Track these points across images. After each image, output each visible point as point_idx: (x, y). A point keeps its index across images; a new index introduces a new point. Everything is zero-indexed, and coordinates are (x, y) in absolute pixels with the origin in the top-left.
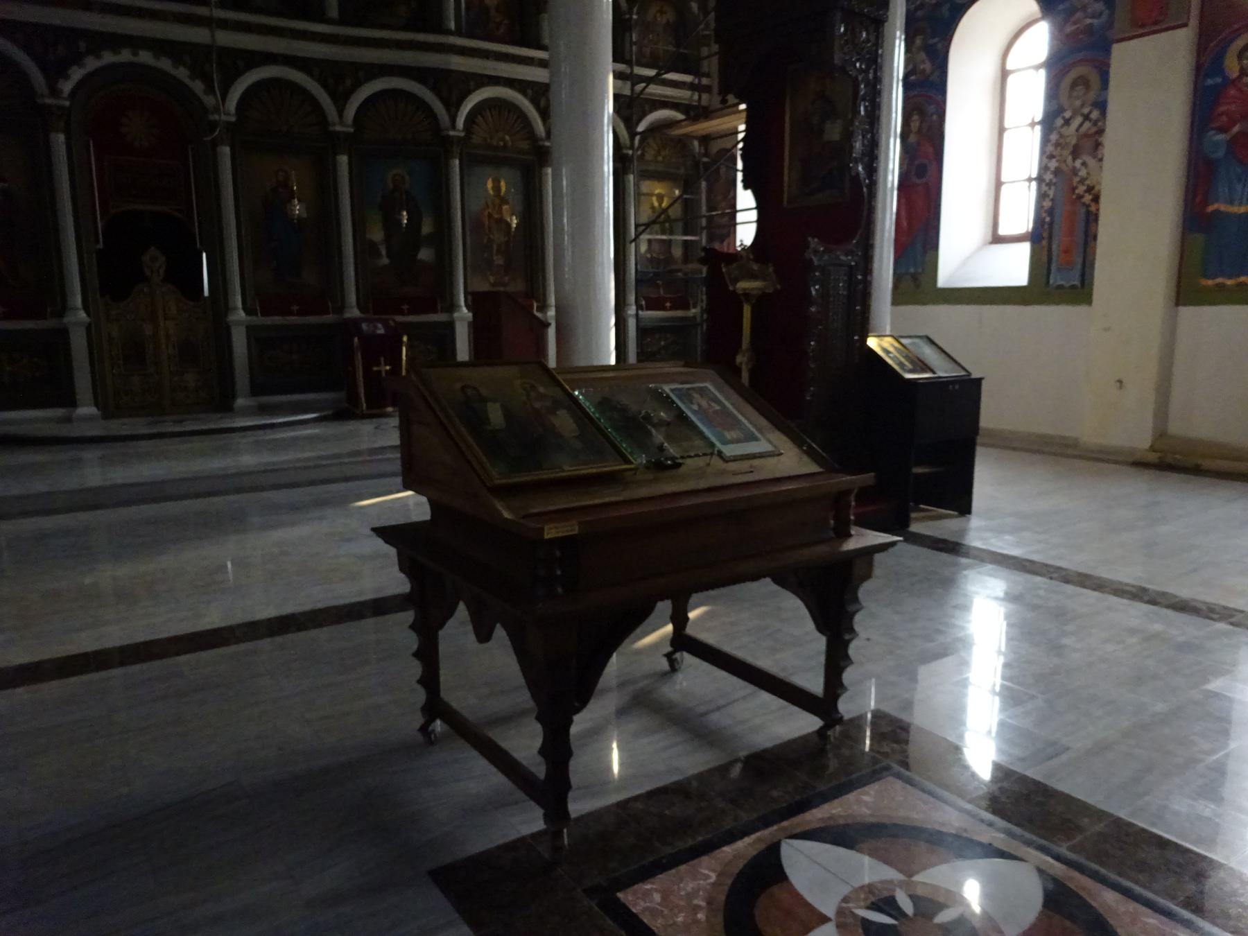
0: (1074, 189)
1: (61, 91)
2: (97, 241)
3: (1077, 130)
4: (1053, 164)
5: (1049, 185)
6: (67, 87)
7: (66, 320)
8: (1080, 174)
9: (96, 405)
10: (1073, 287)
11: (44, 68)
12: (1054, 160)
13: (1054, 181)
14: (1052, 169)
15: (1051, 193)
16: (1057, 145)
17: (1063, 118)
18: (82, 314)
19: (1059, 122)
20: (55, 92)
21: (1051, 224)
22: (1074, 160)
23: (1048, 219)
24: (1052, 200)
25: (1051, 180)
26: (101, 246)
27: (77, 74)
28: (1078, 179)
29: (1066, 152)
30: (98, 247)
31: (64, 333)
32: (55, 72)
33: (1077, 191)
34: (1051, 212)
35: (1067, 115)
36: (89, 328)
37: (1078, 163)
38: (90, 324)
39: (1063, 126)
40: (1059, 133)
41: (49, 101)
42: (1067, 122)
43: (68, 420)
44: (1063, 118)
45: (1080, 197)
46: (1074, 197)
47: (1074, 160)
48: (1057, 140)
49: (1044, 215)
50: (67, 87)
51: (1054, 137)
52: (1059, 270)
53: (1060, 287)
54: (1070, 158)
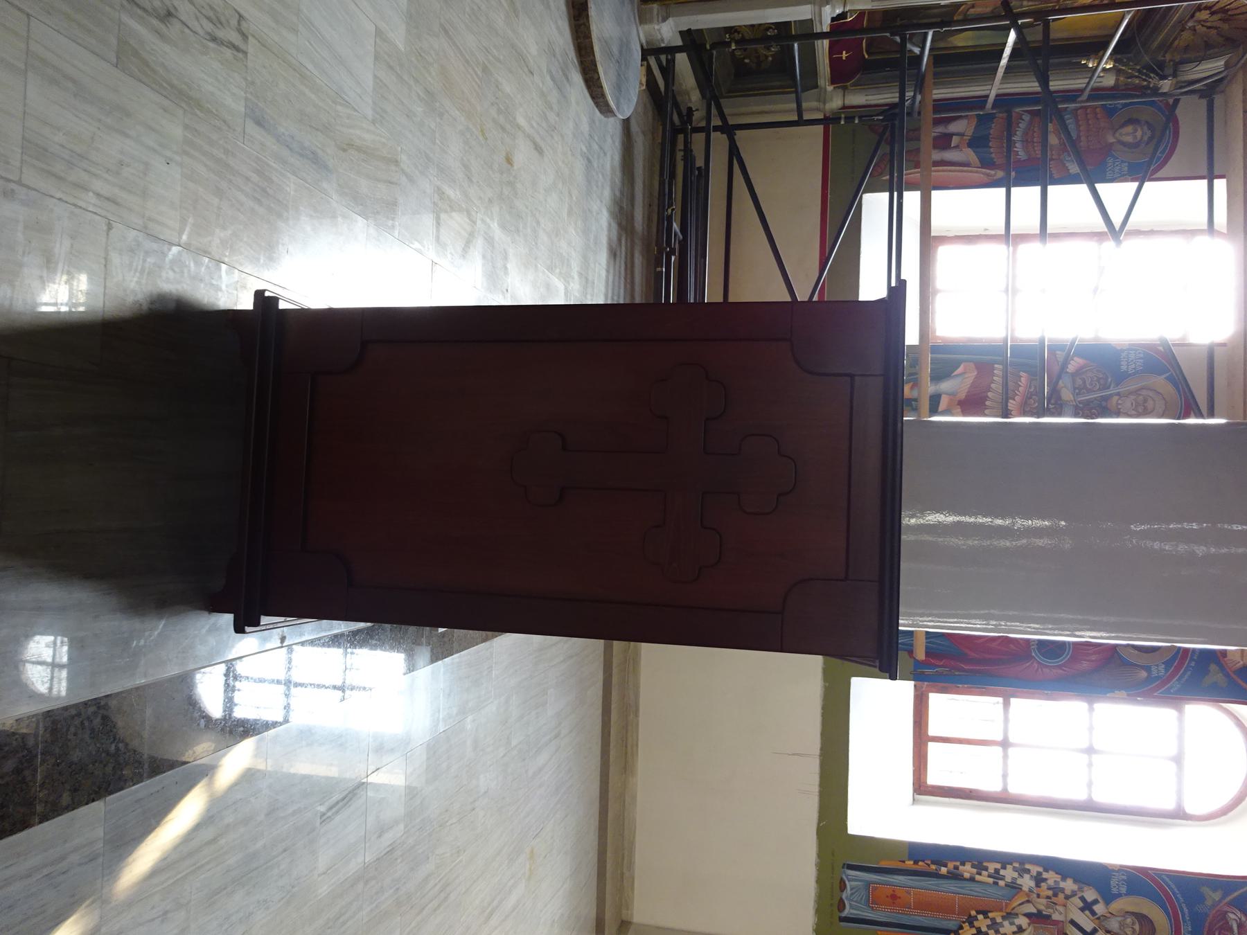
0: (985, 914)
3: (1073, 922)
4: (1027, 882)
5: (996, 875)
8: (1006, 923)
10: (841, 905)
12: (1032, 884)
13: (1001, 883)
14: (1019, 881)
15: (984, 878)
16: (1056, 891)
17: (1096, 902)
19: (1090, 895)
21: (937, 875)
22: (1028, 915)
23: (944, 870)
24: (972, 879)
25: (1003, 878)
28: (999, 920)
29: (1042, 904)
33: (980, 917)
34: (955, 876)
35: (1099, 909)
37: (1023, 921)
39: (1082, 899)
40: (1074, 894)
42: (1087, 907)
44: (1096, 902)
45: (971, 921)
46: (973, 913)
47: (1028, 915)
48: (1062, 890)
49: (951, 865)
51: (1069, 885)
52: (868, 884)
53: (843, 887)
54: (1031, 909)
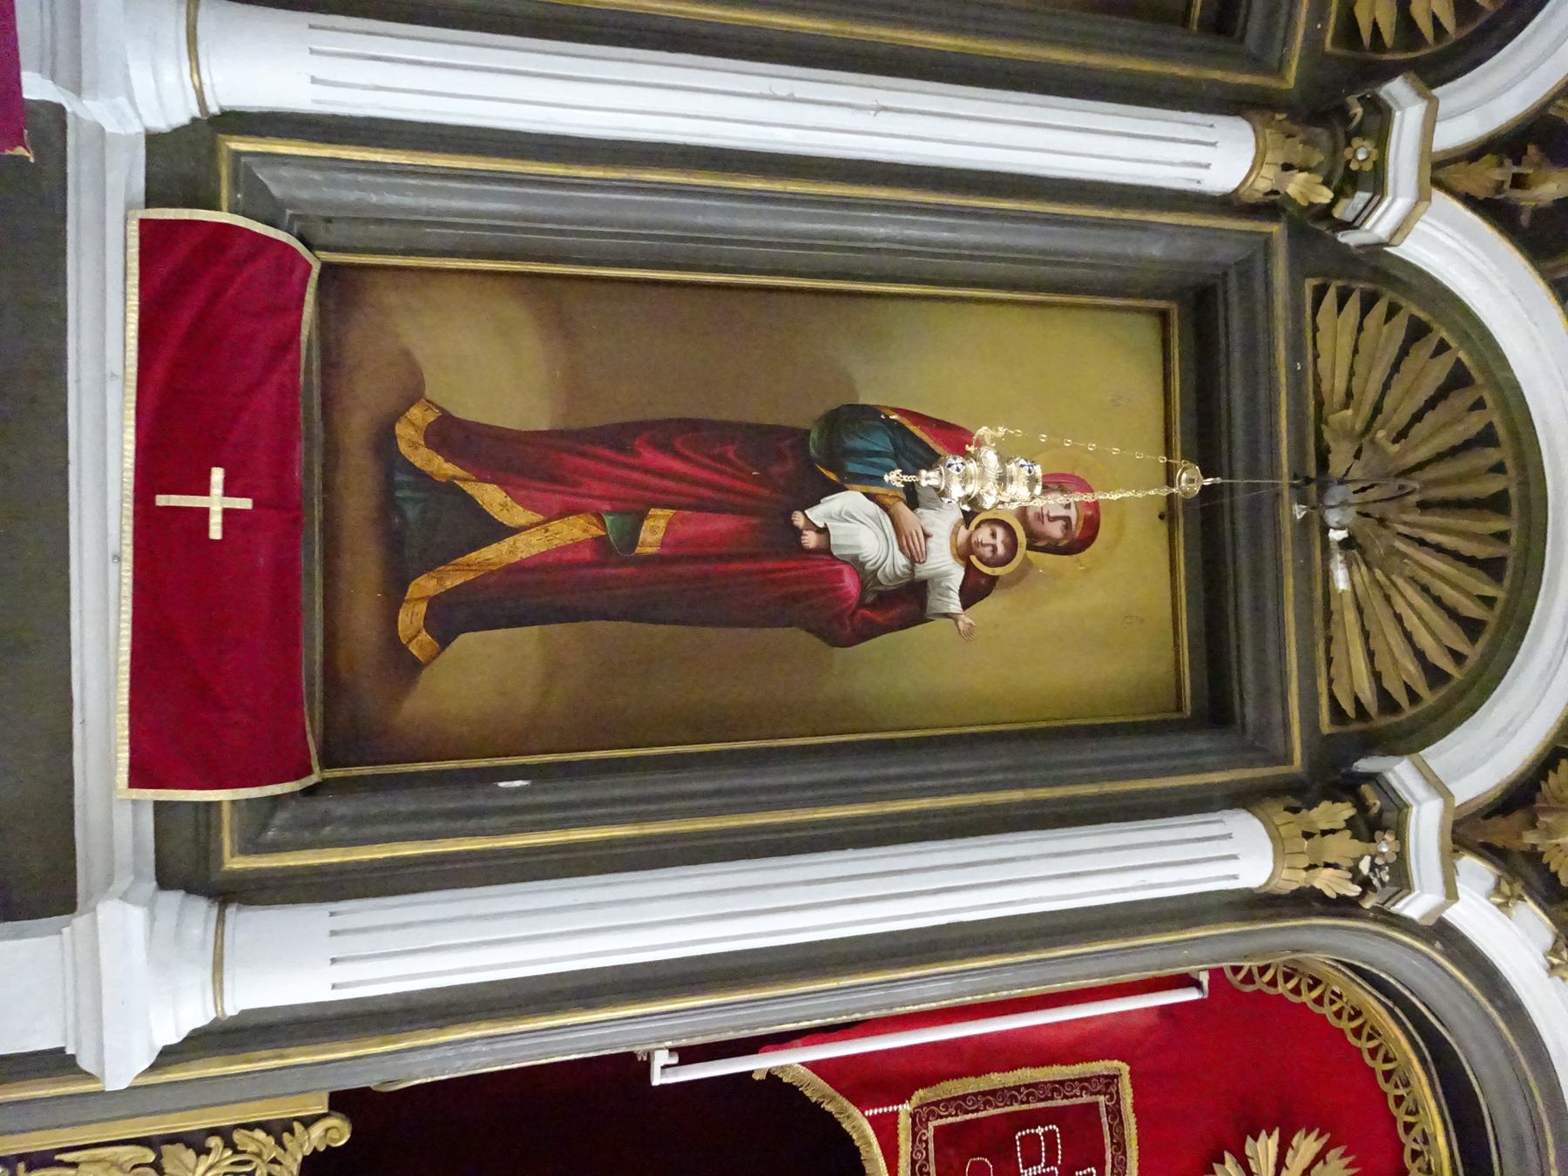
2: (688, 1055)
30: (661, 1058)
36: (57, 1063)
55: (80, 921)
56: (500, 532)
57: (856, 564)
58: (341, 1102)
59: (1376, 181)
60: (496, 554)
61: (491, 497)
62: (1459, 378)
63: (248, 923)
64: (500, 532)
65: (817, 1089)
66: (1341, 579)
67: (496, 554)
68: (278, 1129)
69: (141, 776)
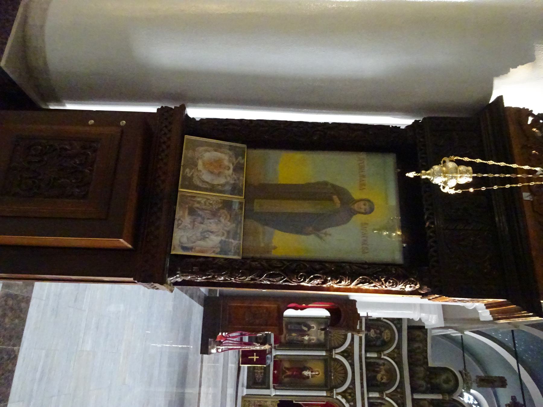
1: (338, 396)
2: (295, 401)
6: (339, 397)
7: (273, 389)
9: (247, 395)
11: (345, 392)
18: (274, 394)
20: (338, 394)
26: (294, 402)
27: (344, 401)
31: (268, 388)
32: (343, 395)
38: (271, 396)
41: (335, 392)
43: (243, 386)
50: (339, 397)
55: (271, 390)
56: (287, 373)
57: (305, 375)
58: (279, 401)
59: (332, 355)
60: (287, 374)
61: (287, 371)
62: (341, 365)
63: (277, 390)
64: (287, 373)
65: (303, 405)
66: (333, 378)
67: (287, 374)
68: (276, 401)
69: (273, 383)
